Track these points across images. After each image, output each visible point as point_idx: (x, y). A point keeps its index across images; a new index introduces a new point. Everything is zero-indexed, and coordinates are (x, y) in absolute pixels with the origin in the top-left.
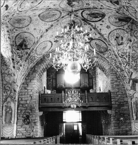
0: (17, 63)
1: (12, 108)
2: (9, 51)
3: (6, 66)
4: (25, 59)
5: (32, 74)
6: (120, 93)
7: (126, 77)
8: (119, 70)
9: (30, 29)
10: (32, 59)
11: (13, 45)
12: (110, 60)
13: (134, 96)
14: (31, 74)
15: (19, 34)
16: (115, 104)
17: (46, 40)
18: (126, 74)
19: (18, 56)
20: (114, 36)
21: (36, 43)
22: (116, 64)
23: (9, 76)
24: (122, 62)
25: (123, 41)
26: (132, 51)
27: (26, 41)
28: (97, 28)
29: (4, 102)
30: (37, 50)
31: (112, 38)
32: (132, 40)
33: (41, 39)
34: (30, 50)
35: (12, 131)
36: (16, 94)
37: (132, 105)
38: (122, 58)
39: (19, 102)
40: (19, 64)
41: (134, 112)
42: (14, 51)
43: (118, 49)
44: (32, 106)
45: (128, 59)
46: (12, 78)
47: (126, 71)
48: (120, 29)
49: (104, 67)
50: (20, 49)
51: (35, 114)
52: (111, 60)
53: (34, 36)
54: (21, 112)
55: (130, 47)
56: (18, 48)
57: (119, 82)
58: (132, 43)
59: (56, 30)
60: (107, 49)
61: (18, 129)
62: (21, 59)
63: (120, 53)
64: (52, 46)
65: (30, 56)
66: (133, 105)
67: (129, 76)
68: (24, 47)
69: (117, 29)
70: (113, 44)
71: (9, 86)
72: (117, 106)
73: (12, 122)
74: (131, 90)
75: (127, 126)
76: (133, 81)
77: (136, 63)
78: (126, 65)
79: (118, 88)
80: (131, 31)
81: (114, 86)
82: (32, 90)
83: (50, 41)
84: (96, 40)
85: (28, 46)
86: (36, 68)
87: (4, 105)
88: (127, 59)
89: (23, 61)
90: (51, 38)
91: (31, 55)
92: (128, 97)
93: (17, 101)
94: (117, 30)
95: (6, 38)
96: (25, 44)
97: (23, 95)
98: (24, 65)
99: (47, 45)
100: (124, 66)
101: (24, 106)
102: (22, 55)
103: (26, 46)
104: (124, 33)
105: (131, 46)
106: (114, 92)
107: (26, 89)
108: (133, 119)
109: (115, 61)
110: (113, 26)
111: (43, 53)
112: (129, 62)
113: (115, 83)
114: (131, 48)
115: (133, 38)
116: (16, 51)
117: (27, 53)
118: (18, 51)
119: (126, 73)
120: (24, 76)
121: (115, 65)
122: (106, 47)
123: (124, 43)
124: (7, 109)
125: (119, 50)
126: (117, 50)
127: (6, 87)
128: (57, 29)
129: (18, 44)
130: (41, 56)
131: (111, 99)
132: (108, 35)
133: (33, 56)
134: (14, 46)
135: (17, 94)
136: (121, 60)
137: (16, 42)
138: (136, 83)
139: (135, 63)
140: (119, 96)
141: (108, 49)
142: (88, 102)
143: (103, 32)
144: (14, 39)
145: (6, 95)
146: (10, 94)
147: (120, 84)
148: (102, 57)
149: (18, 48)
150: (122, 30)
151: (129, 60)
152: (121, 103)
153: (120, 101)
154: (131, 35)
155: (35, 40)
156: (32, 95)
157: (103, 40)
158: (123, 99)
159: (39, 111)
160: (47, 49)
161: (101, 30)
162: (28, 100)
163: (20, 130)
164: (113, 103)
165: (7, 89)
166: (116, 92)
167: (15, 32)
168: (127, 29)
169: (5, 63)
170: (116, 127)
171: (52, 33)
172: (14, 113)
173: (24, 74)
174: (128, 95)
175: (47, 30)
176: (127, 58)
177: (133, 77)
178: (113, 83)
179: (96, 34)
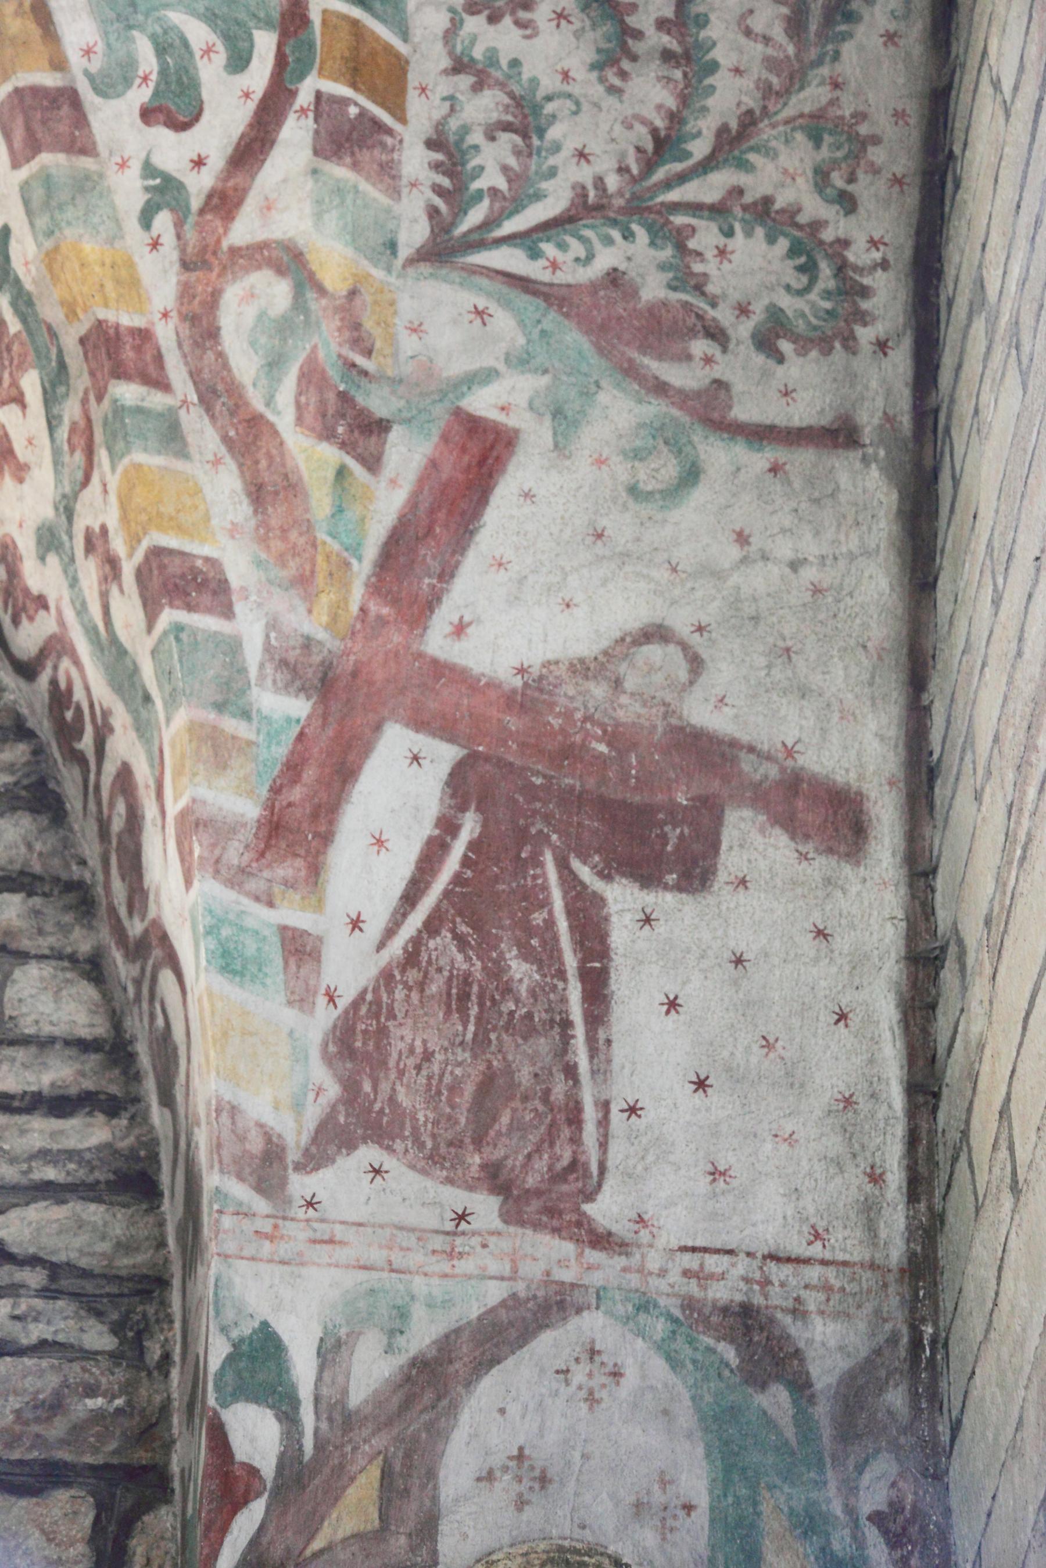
13: (457, 1467)
18: (223, 489)
47: (244, 364)
74: (342, 1185)
76: (461, 786)
77: (651, 92)
78: (252, 149)
100: (164, 191)
119: (203, 433)
138: (622, 899)
139: (616, 56)
177: (518, 611)
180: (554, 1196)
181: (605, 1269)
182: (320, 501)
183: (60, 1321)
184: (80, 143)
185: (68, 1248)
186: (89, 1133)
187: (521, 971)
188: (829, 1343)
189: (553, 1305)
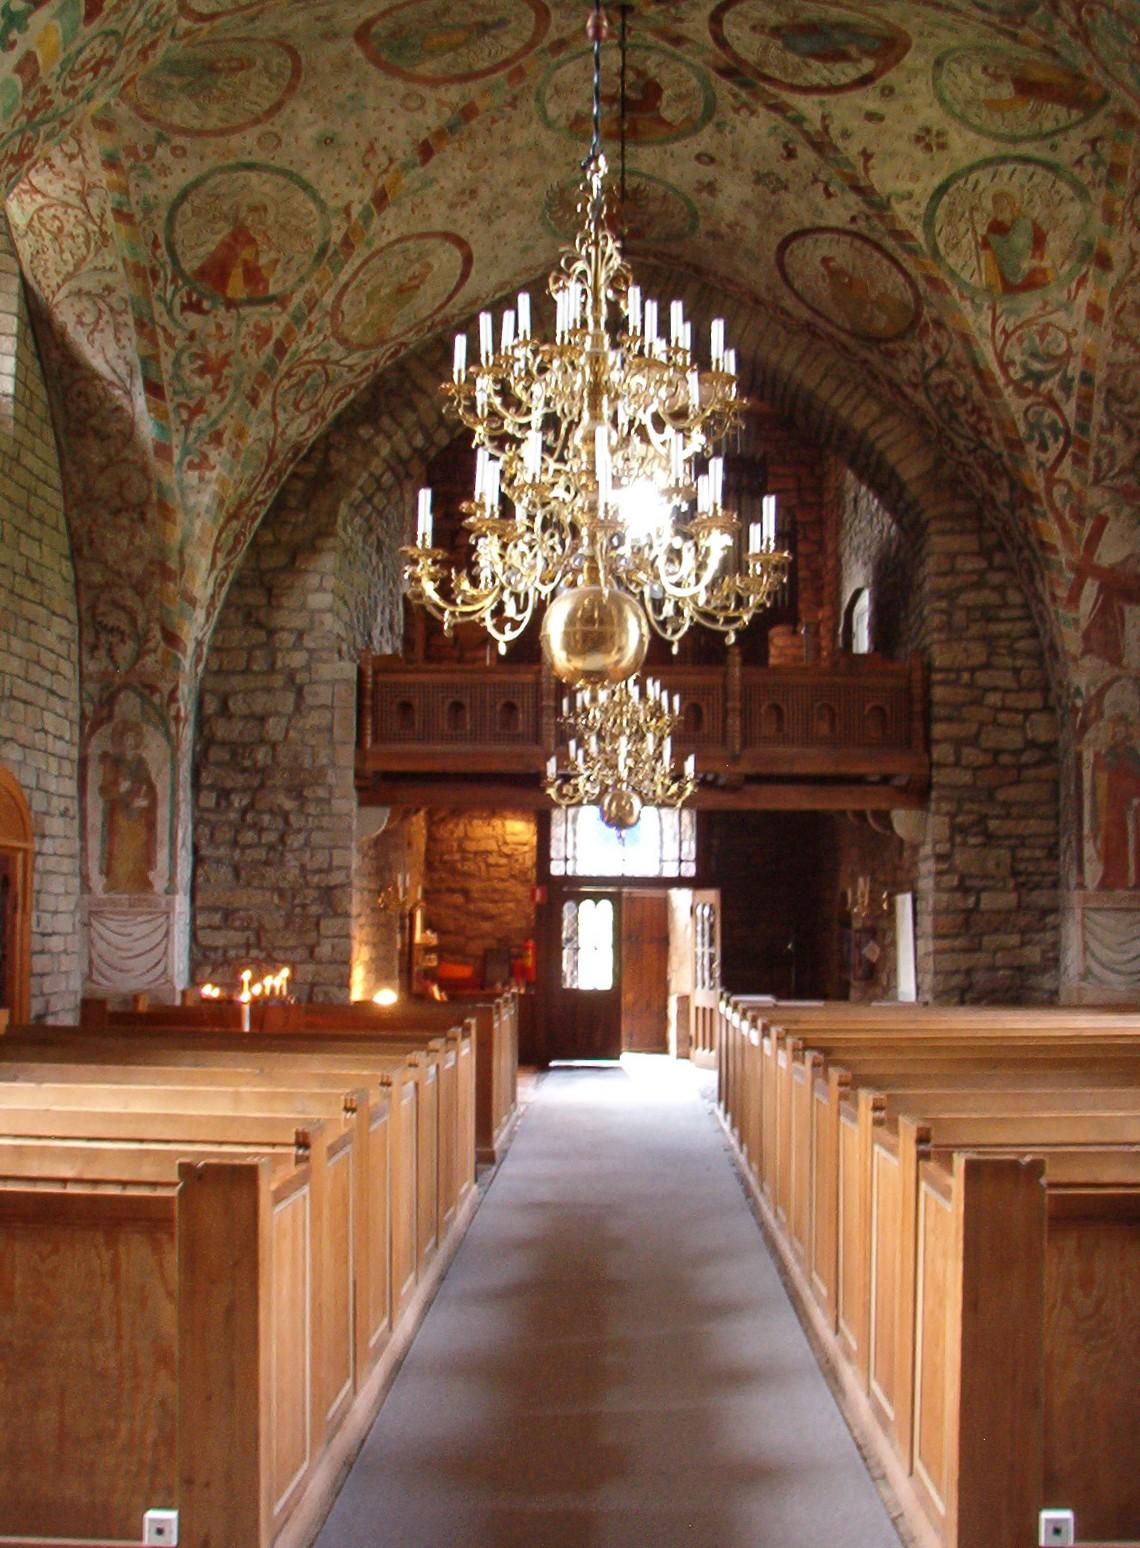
0: (185, 415)
1: (153, 770)
2: (121, 319)
3: (103, 440)
4: (247, 385)
5: (308, 505)
6: (1006, 680)
7: (1054, 549)
8: (1002, 495)
9: (284, 140)
10: (302, 382)
11: (155, 276)
12: (938, 409)
13: (1106, 702)
14: (292, 502)
15: (196, 185)
16: (957, 764)
17: (421, 228)
18: (1055, 528)
19: (195, 356)
20: (977, 216)
21: (335, 252)
22: (982, 445)
23: (124, 520)
24: (1032, 427)
25: (1042, 257)
26: (1115, 348)
27: (252, 241)
28: (840, 143)
29: (93, 731)
30: (345, 306)
31: (962, 229)
32: (1118, 253)
33: (376, 223)
34: (284, 308)
35: (162, 946)
36: (178, 666)
37: (1079, 777)
38: (1029, 401)
39: (206, 732)
40: (200, 422)
41: (1095, 829)
42: (165, 320)
43: (1001, 321)
44: (307, 763)
45: (1079, 407)
46: (145, 538)
47: (1059, 504)
48: (1026, 160)
49: (892, 457)
50: (206, 305)
51: (325, 822)
52: (944, 410)
53: (323, 196)
54: (218, 804)
55: (1094, 313)
56: (194, 297)
57: (1000, 589)
58: (1112, 279)
59: (505, 147)
60: (918, 314)
61: (206, 938)
62: (217, 382)
63: (1015, 353)
64: (465, 276)
65: (287, 357)
66: (1087, 773)
67: (1072, 549)
68: (237, 287)
69: (1003, 160)
70: (965, 276)
71: (130, 598)
72: (966, 778)
73: (159, 879)
74: (1087, 662)
75: (1028, 936)
79: (987, 639)
80: (1109, 185)
81: (960, 617)
82: (301, 634)
83: (447, 236)
84: (828, 236)
85: (271, 281)
86: (333, 453)
87: (95, 748)
88: (1070, 408)
89: (233, 400)
90: (460, 215)
91: (294, 353)
92: (1060, 712)
93: (186, 719)
94: (1001, 168)
95: (95, 212)
96: (245, 263)
97: (233, 673)
98: (240, 434)
99: (429, 266)
100: (1041, 465)
101: (247, 763)
102: (226, 356)
103: (253, 275)
104: (1058, 192)
105: (1104, 303)
106: (959, 671)
107: (259, 625)
108: (1081, 886)
109: (973, 419)
110: (971, 136)
111: (395, 330)
112: (1083, 428)
113: (966, 598)
114: (1106, 318)
115: (1126, 244)
116: (180, 319)
117: (262, 336)
118: (194, 320)
119: (1051, 516)
120: (243, 518)
121: (972, 446)
122: (909, 296)
123: (1051, 275)
124: (116, 783)
125: (1010, 328)
126: (998, 330)
127: (102, 608)
128: (506, 139)
129: (190, 264)
130: (375, 354)
131: (928, 720)
132: (924, 205)
133: (314, 356)
134: (160, 284)
135: (187, 663)
136: (1019, 416)
137: (179, 250)
138: (1127, 609)
140: (994, 699)
141: (927, 313)
142: (746, 742)
143: (884, 178)
144: (161, 224)
145: (104, 674)
146: (135, 663)
147: (1005, 605)
148: (875, 378)
149: (194, 297)
150: (1040, 171)
151: (1084, 412)
152: (1005, 759)
153: (990, 739)
154: (1110, 217)
155: (327, 231)
156: (300, 678)
157: (889, 243)
159: (362, 803)
160: (425, 302)
161: (873, 161)
162: (277, 713)
163: (219, 939)
164: (940, 752)
165: (111, 621)
166: (973, 670)
167: (165, 170)
168: (1079, 162)
169: (91, 414)
170: (946, 943)
171: (468, 174)
172: (168, 816)
173: (241, 505)
174: (1059, 698)
175: (426, 151)
176: (1068, 398)
177: (1108, 554)
178: (950, 595)
179: (831, 189)
180: (1116, 660)
182: (1075, 534)
184: (1022, 448)
186: (1027, 626)
187: (1111, 623)
189: (1117, 679)
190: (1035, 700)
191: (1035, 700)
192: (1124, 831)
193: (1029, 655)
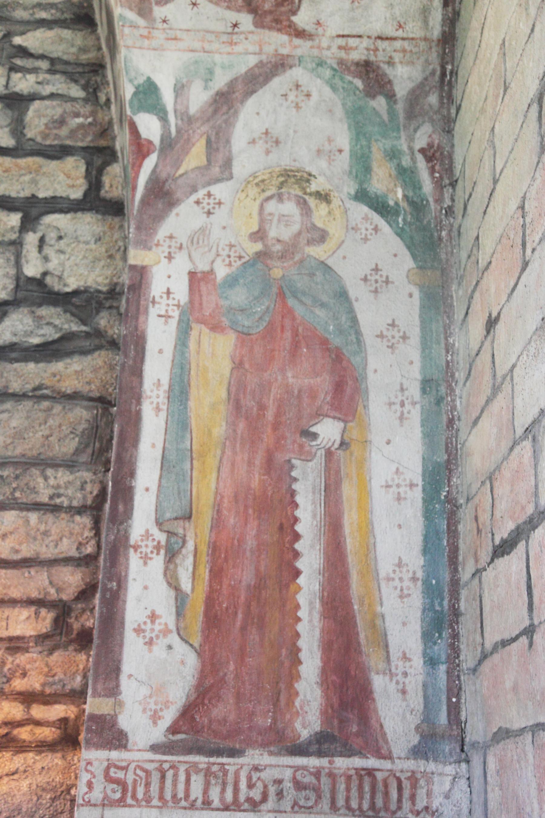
41: (175, 522)
158: (17, 245)
181: (302, 47)
183: (58, 84)
185: (57, 51)
188: (404, 76)
189: (279, 65)
190: (66, 178)
191: (66, 178)
192: (288, 532)
193: (56, 65)
